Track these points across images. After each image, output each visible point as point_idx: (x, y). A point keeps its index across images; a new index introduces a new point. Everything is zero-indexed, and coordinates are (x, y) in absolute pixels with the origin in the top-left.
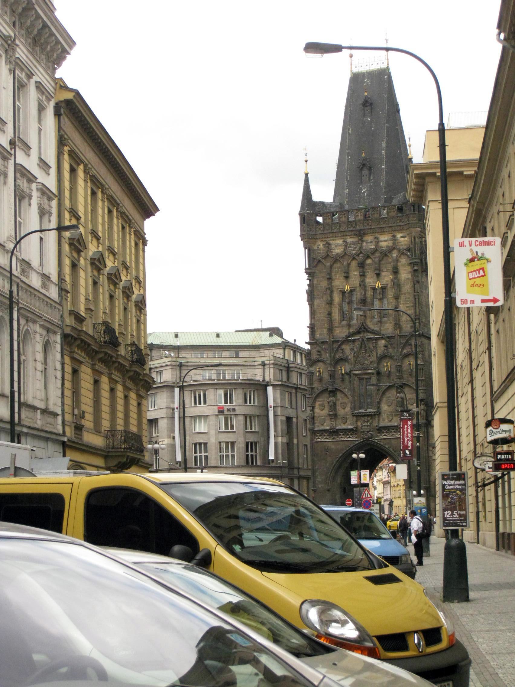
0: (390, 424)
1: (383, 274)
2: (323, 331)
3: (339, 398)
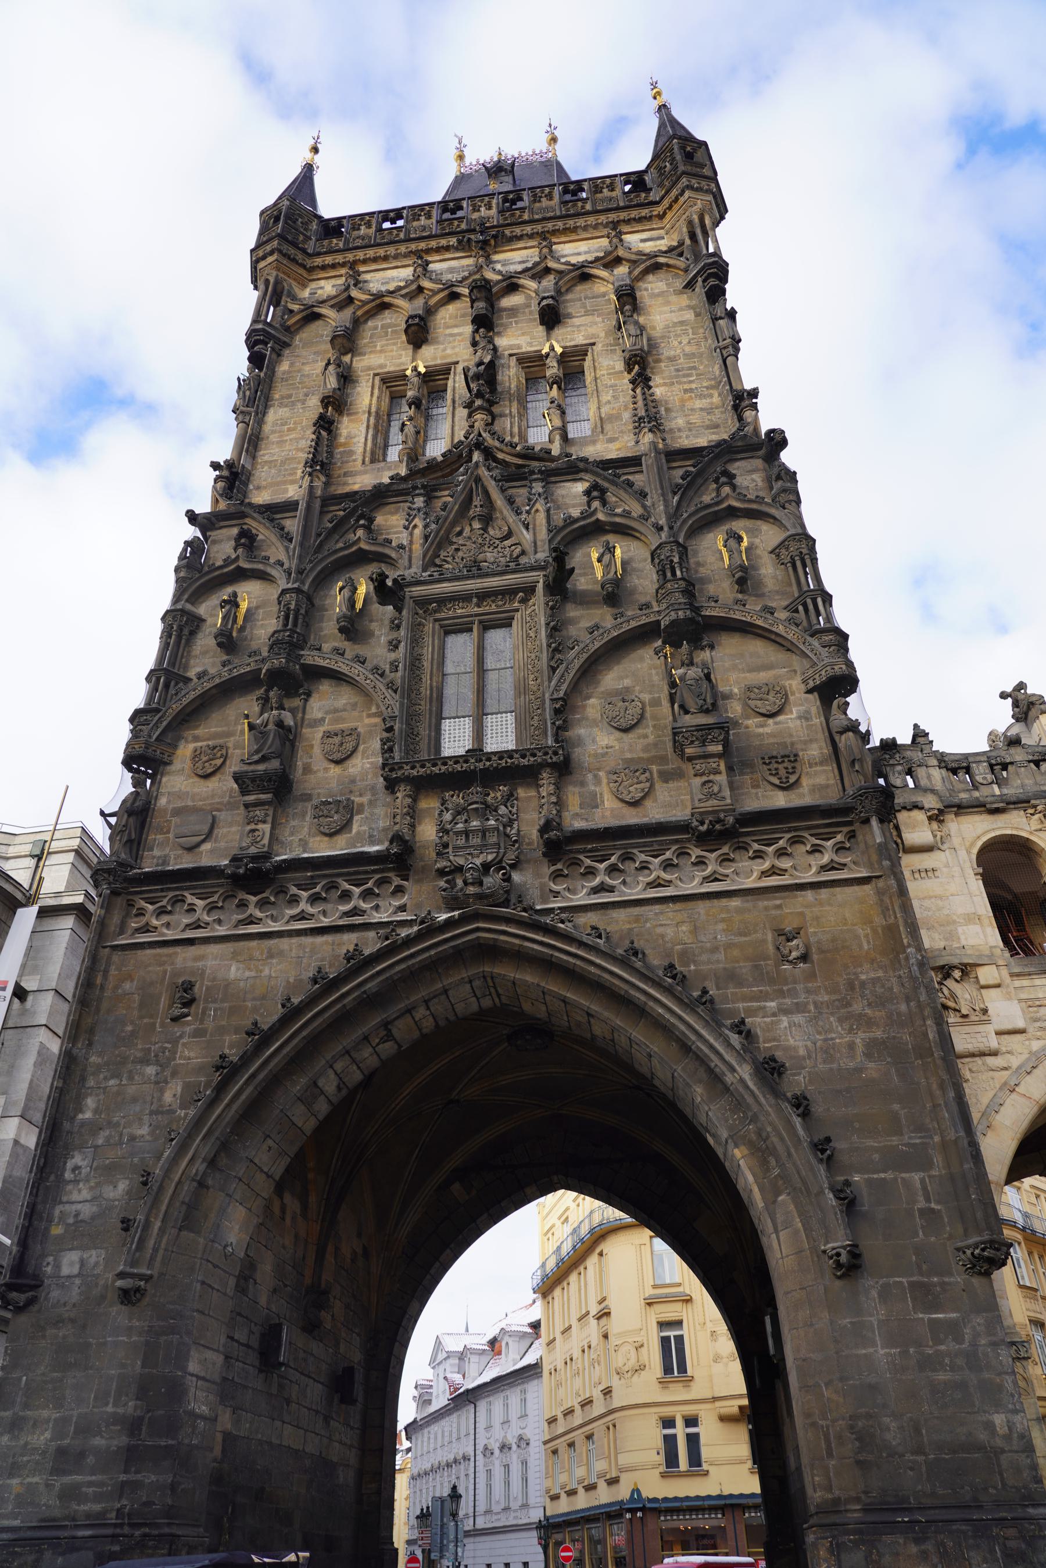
3: (320, 715)
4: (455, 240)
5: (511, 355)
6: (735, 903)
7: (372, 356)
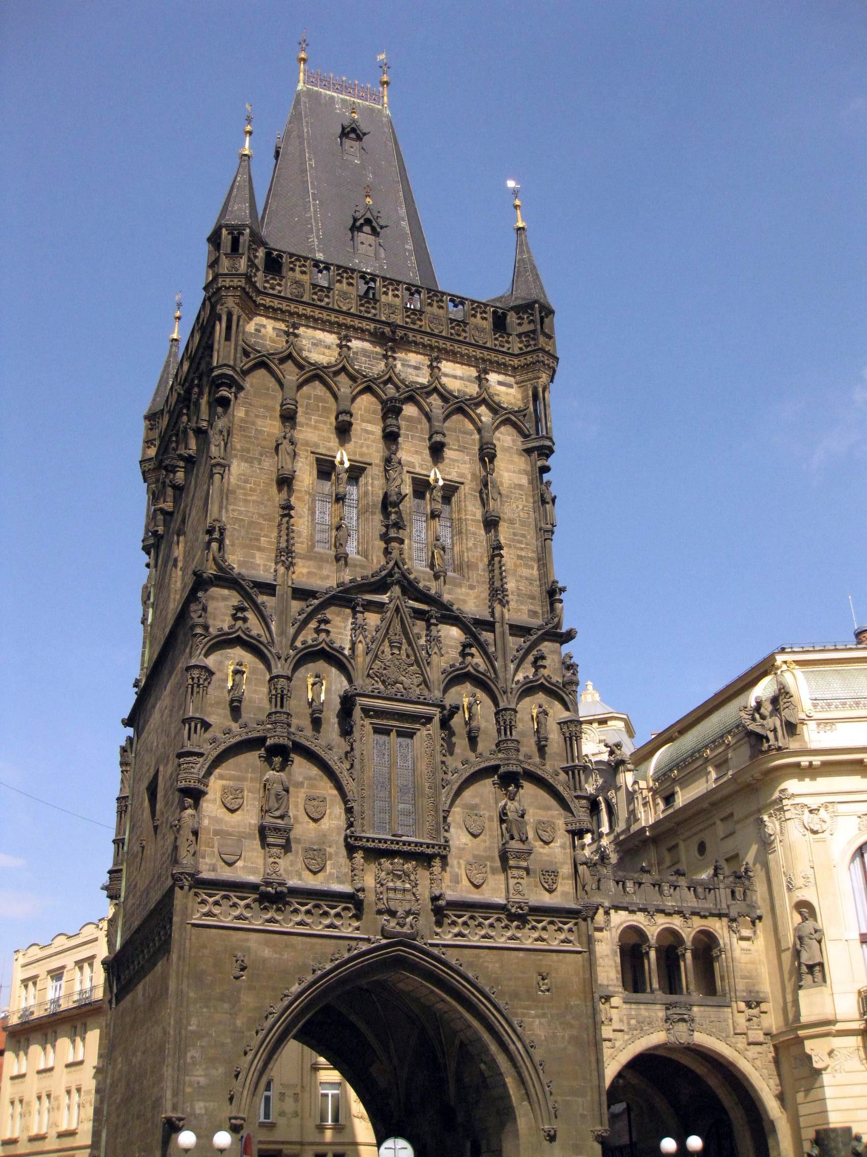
0: (475, 896)
1: (448, 453)
2: (253, 557)
3: (301, 779)
4: (373, 326)
5: (408, 472)
6: (521, 954)
7: (309, 430)
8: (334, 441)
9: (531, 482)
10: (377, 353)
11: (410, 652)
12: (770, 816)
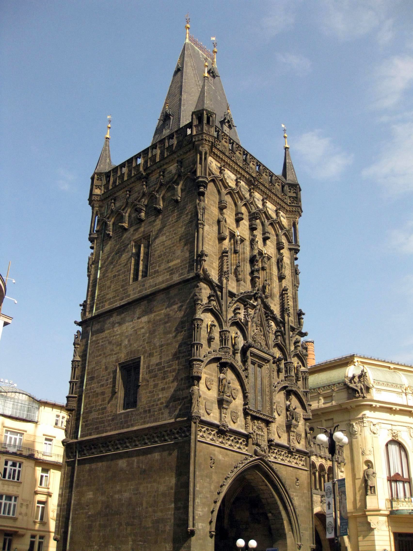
6: (291, 469)
8: (235, 226)
9: (291, 263)
10: (247, 189)
11: (262, 329)
12: (356, 424)
